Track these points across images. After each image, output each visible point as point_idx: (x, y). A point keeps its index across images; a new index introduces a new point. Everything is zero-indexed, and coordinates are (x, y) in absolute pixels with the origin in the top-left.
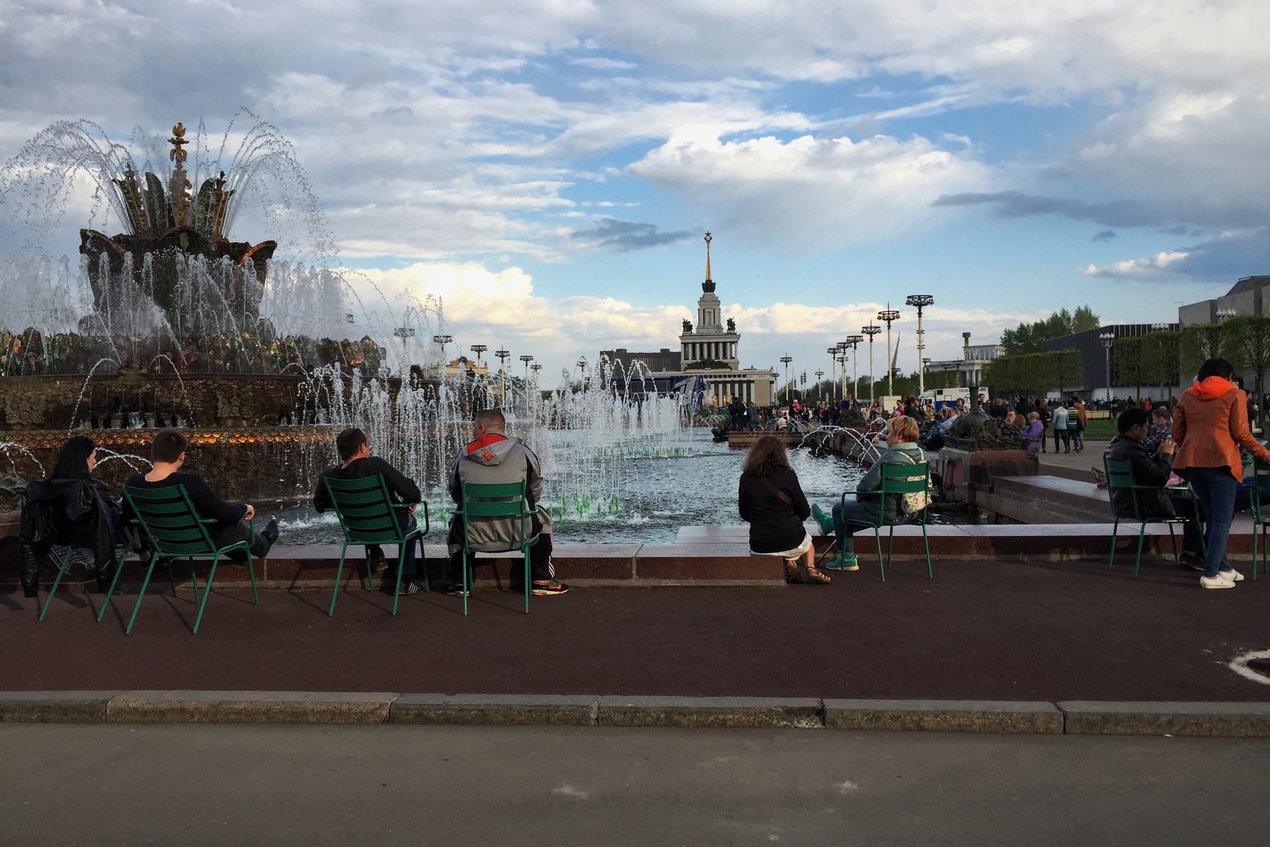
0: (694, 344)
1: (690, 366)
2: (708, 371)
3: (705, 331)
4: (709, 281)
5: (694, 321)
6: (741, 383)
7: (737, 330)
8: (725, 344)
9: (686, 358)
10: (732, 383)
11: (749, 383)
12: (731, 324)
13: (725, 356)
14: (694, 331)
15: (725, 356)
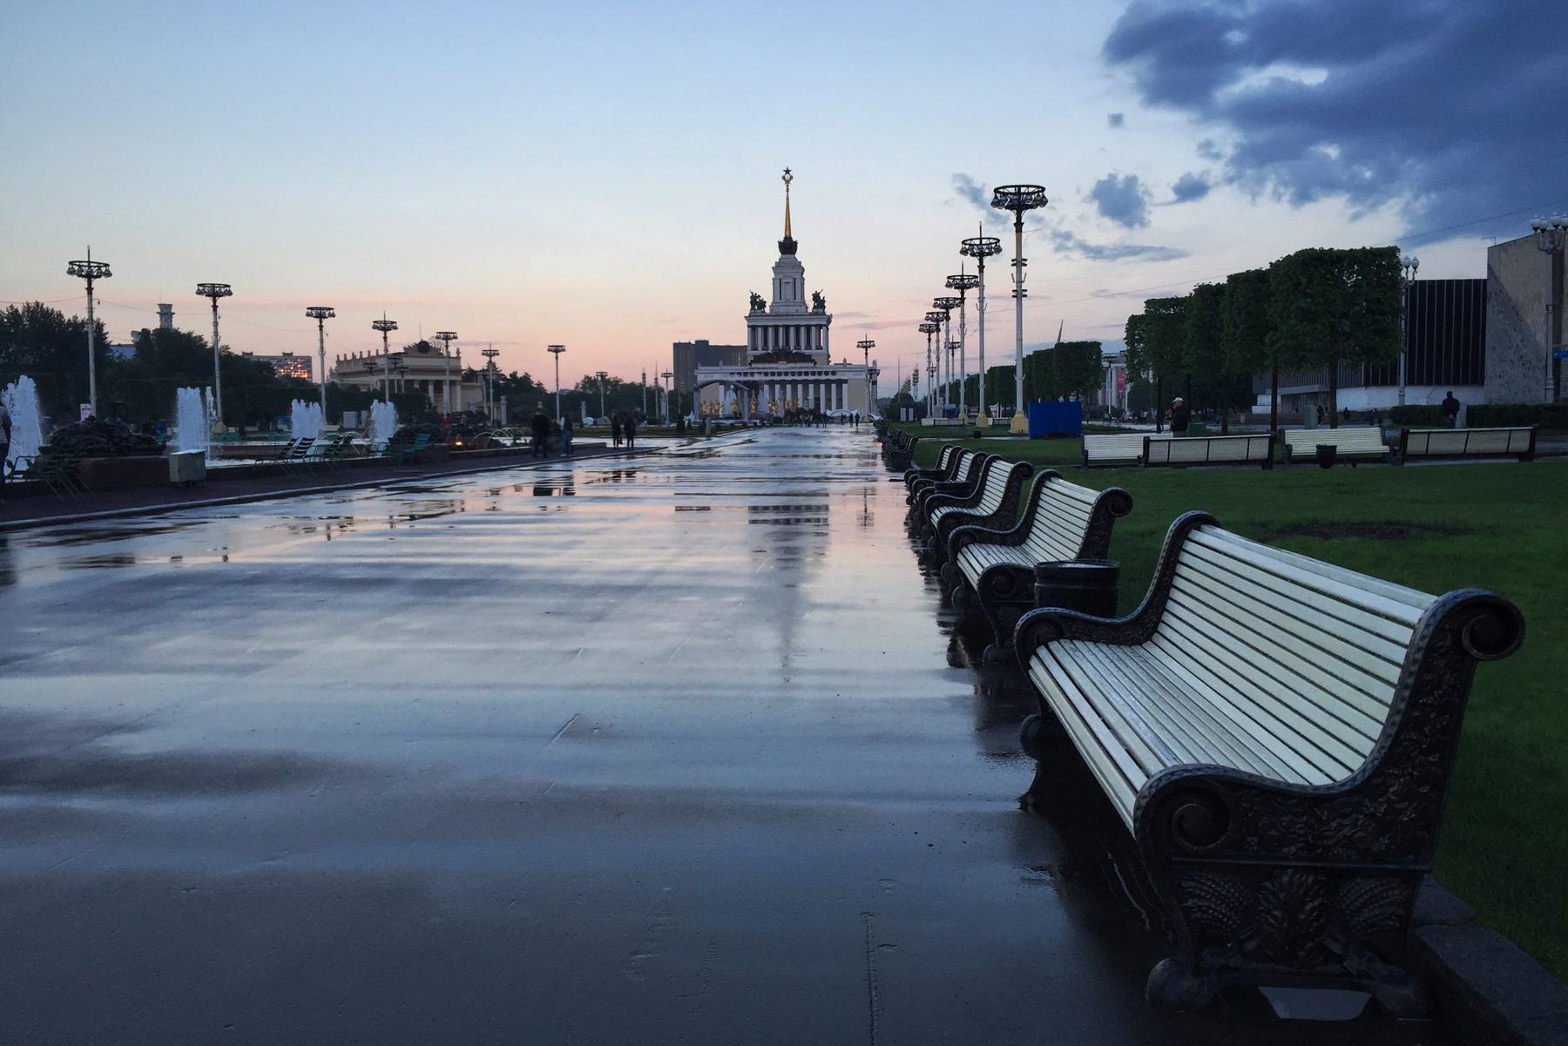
0: (765, 328)
1: (758, 359)
2: (783, 366)
3: (782, 310)
4: (788, 238)
5: (768, 296)
6: (828, 383)
7: (828, 311)
8: (808, 327)
9: (755, 348)
10: (817, 383)
11: (840, 383)
12: (819, 301)
13: (808, 346)
14: (767, 310)
15: (808, 346)
